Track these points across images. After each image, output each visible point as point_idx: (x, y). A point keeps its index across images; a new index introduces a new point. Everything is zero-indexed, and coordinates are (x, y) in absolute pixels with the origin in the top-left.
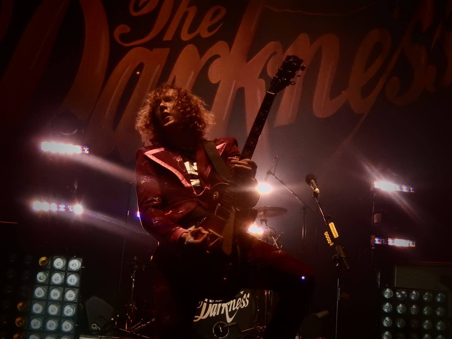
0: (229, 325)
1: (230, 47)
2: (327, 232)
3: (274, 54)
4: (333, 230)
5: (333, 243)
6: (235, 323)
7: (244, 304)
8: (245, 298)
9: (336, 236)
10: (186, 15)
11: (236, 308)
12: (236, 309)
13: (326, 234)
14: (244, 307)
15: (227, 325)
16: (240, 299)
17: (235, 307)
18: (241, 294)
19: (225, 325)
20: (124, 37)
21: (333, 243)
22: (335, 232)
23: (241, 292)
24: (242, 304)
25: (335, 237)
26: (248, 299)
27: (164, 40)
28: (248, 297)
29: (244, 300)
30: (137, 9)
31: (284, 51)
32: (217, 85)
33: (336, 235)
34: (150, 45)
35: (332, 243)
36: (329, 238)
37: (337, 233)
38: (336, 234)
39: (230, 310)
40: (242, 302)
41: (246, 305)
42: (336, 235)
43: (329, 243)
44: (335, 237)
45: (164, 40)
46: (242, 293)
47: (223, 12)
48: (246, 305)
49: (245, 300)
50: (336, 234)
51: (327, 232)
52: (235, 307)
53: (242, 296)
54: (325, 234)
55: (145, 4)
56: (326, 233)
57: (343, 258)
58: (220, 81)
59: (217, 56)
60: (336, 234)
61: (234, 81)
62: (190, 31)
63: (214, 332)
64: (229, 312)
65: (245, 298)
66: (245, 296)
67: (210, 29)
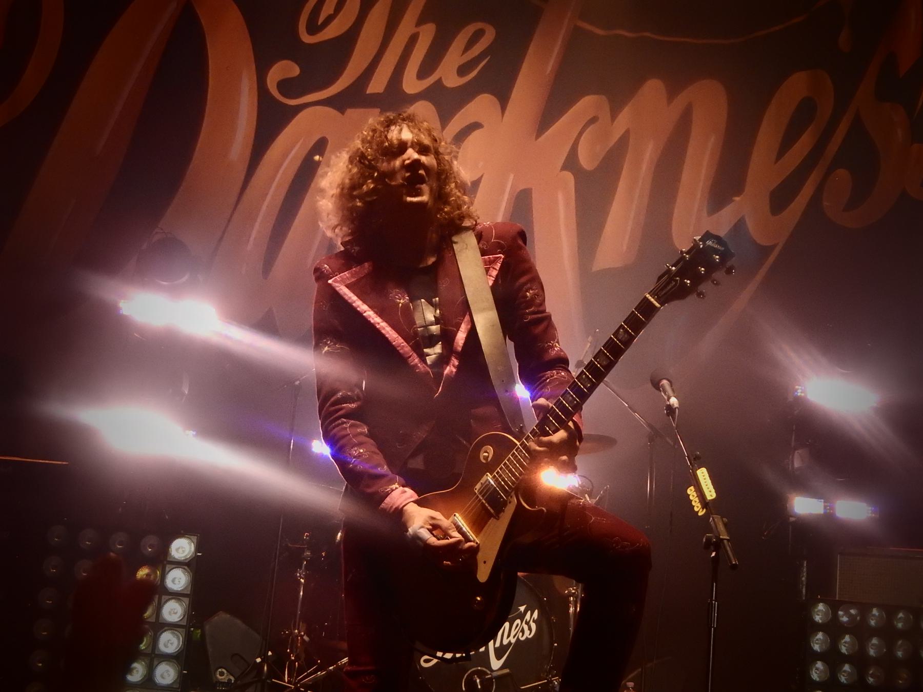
0: (495, 674)
1: (503, 108)
2: (692, 488)
3: (593, 120)
4: (706, 484)
5: (705, 510)
6: (506, 671)
7: (527, 632)
8: (528, 620)
9: (711, 496)
10: (413, 40)
11: (510, 641)
12: (510, 643)
13: (691, 492)
14: (527, 637)
15: (491, 674)
16: (518, 621)
17: (507, 638)
18: (521, 611)
19: (488, 674)
20: (286, 86)
21: (705, 510)
22: (708, 488)
23: (520, 608)
24: (523, 631)
25: (709, 498)
26: (534, 621)
27: (368, 92)
28: (534, 618)
30: (313, 28)
31: (614, 117)
32: (476, 184)
33: (711, 493)
34: (340, 103)
35: (703, 511)
36: (697, 499)
37: (713, 491)
38: (710, 491)
39: (498, 645)
40: (523, 628)
41: (530, 634)
42: (711, 493)
43: (696, 509)
44: (709, 498)
45: (368, 92)
46: (522, 608)
47: (490, 34)
48: (530, 634)
49: (527, 623)
50: (710, 491)
51: (692, 488)
52: (507, 638)
53: (522, 616)
54: (689, 492)
55: (329, 19)
56: (691, 490)
57: (725, 542)
58: (482, 176)
59: (476, 126)
60: (710, 493)
61: (512, 176)
62: (421, 75)
63: (464, 689)
64: (496, 650)
65: (528, 620)
67: (462, 70)
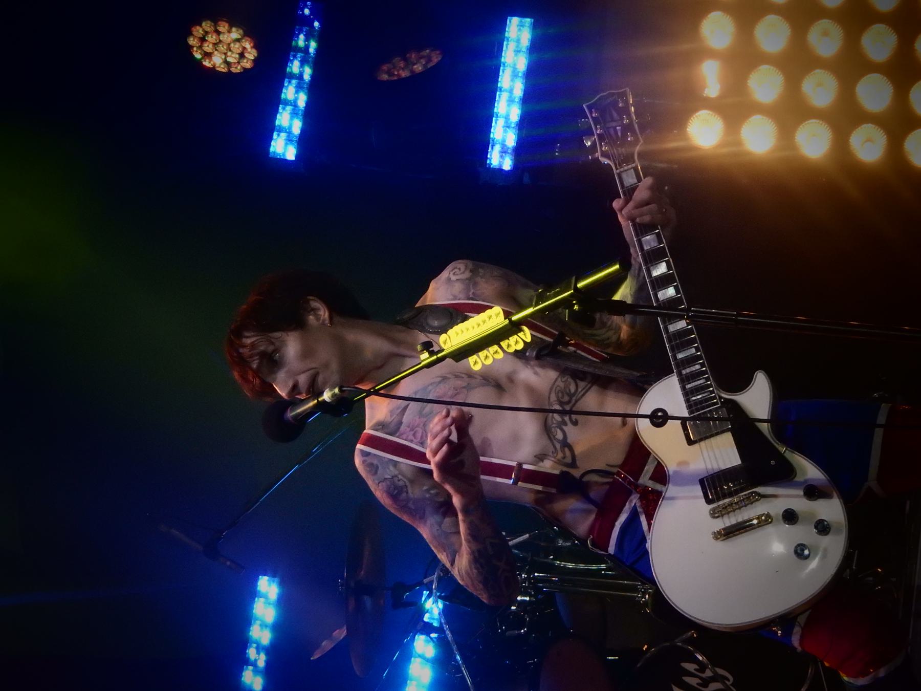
5: (525, 328)
8: (700, 681)
9: (497, 315)
22: (484, 322)
26: (704, 672)
29: (706, 686)
33: (494, 317)
42: (494, 317)
48: (729, 680)
50: (490, 317)
65: (700, 681)
66: (693, 681)
